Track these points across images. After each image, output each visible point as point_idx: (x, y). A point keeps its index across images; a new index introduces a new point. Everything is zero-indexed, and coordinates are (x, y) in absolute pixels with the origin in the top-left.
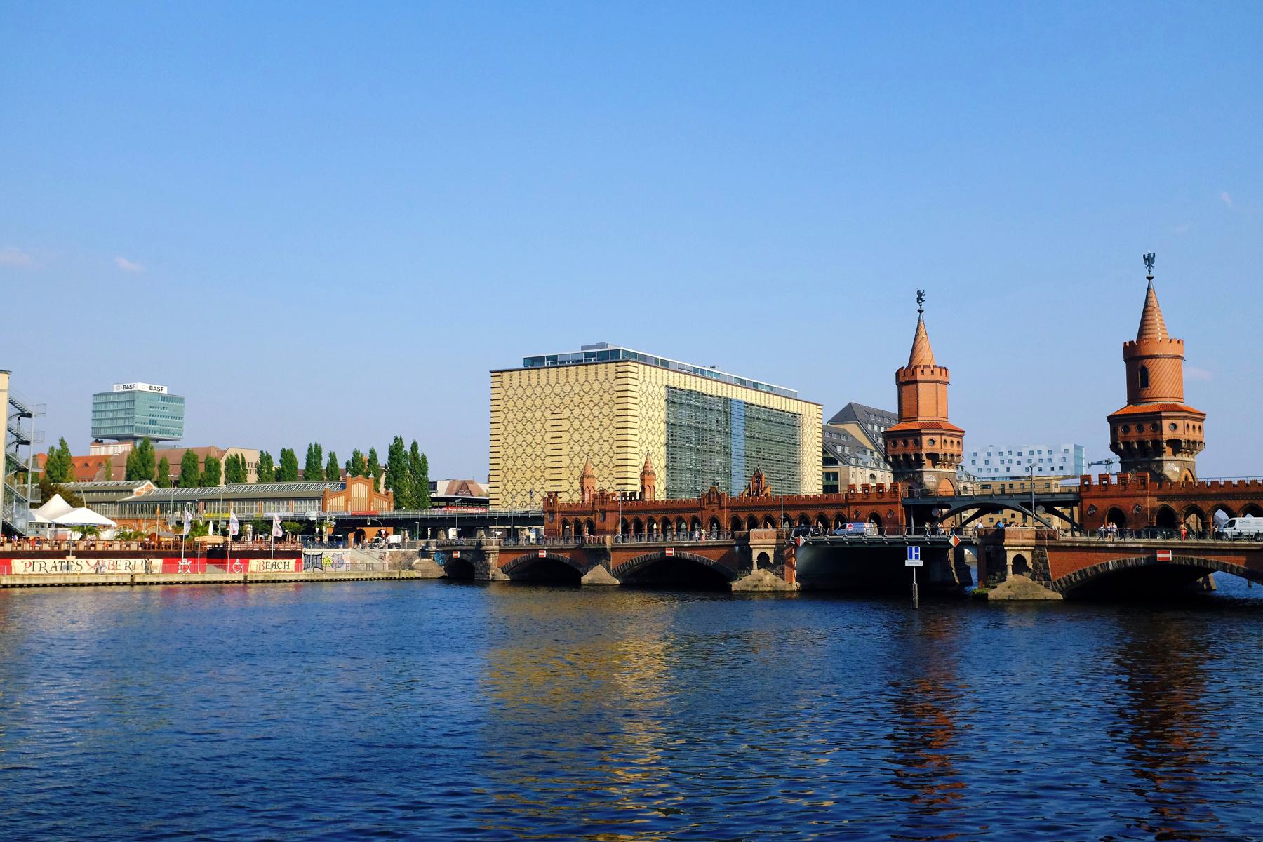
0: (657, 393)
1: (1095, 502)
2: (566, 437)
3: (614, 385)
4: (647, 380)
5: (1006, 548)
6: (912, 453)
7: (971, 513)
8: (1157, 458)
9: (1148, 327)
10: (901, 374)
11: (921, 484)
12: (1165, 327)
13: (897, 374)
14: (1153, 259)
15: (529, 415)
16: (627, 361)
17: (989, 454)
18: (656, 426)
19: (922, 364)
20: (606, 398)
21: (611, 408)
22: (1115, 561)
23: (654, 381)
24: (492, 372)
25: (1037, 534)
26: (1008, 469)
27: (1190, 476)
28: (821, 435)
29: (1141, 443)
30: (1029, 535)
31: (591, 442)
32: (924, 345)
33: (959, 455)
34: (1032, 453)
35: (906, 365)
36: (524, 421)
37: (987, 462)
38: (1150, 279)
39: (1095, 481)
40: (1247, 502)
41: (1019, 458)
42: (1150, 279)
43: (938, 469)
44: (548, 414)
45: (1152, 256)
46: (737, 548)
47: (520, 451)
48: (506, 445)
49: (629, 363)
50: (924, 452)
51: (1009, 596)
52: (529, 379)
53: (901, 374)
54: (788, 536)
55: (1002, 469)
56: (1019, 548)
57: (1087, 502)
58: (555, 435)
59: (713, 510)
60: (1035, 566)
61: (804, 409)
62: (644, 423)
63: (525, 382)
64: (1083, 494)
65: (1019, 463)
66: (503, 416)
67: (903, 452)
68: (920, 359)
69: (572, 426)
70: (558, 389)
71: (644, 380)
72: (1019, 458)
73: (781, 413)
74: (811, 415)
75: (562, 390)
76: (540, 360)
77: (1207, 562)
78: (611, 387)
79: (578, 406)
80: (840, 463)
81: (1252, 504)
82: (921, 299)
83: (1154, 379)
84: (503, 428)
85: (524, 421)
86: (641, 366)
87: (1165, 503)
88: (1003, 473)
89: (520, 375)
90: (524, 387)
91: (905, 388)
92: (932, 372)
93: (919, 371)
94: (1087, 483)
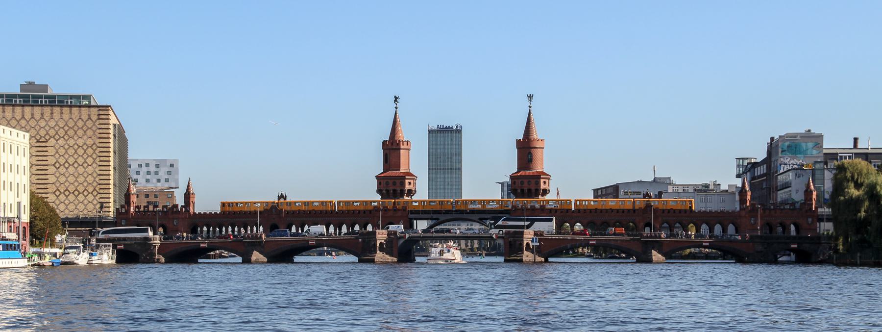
2: (51, 160)
3: (97, 123)
6: (399, 189)
12: (538, 133)
25: (535, 233)
34: (140, 166)
35: (387, 139)
38: (530, 107)
42: (530, 107)
46: (360, 240)
59: (274, 219)
69: (57, 152)
78: (94, 125)
79: (63, 137)
82: (397, 101)
90: (9, 119)
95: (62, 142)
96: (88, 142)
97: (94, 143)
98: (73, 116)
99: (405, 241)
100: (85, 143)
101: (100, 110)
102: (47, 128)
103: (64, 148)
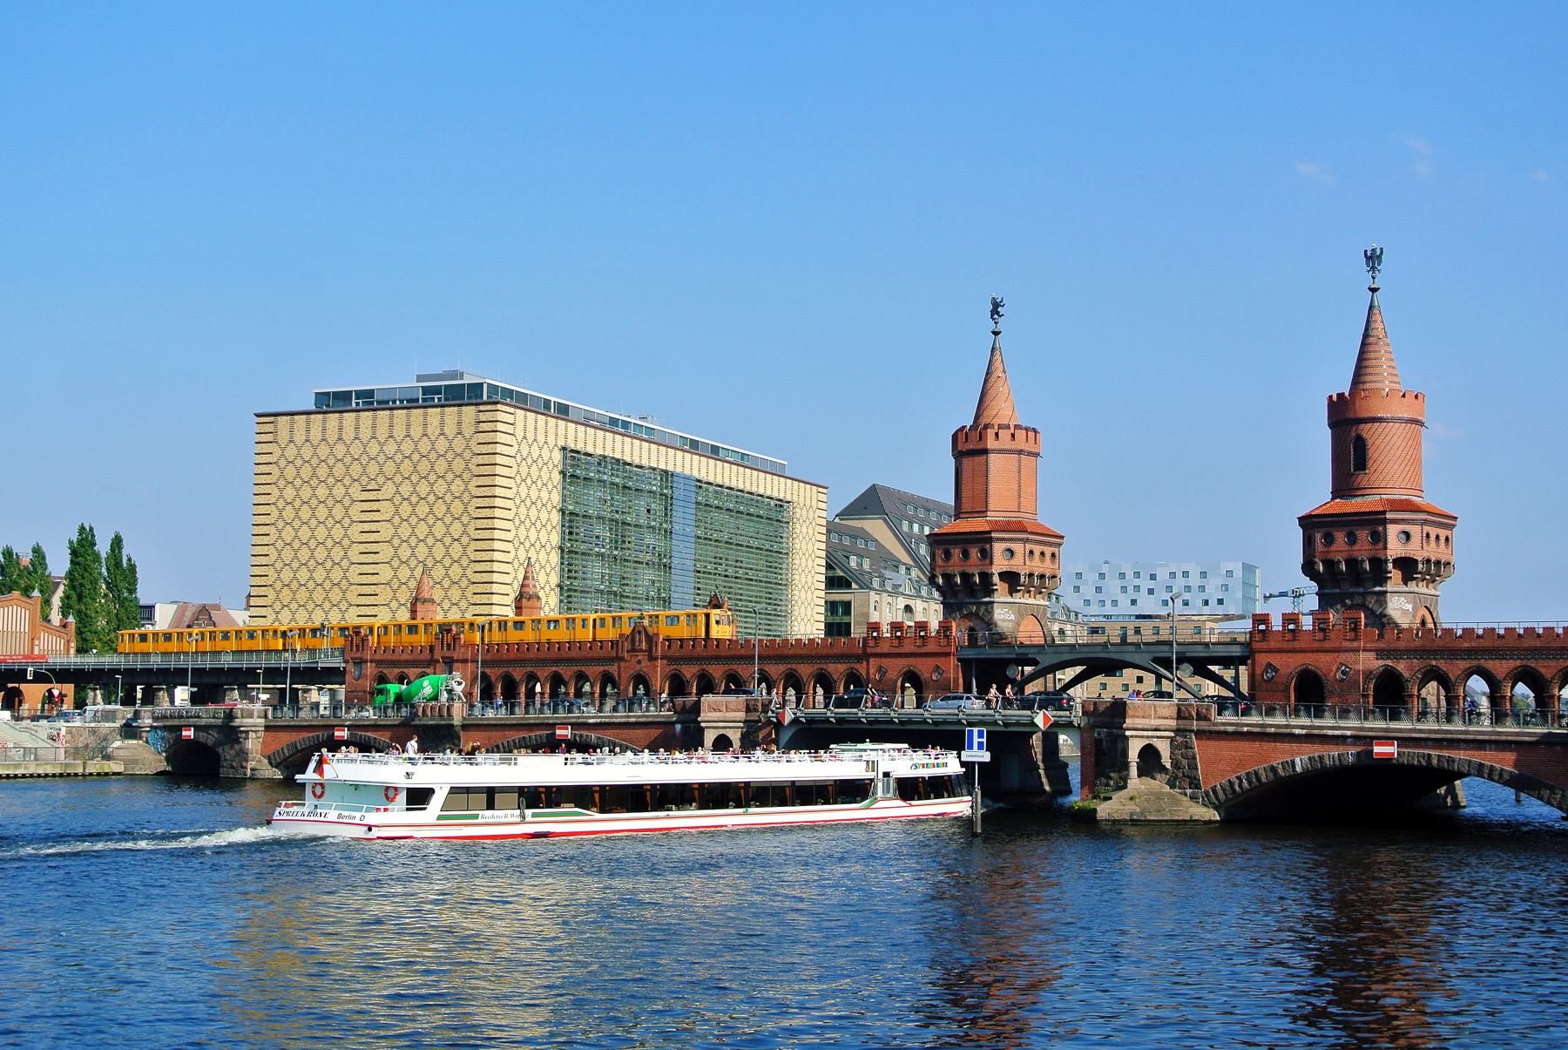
0: (546, 460)
1: (1276, 660)
2: (386, 531)
3: (473, 444)
4: (531, 437)
5: (1128, 733)
6: (976, 572)
7: (1069, 674)
8: (1378, 589)
9: (1368, 371)
10: (961, 438)
11: (990, 624)
13: (955, 437)
14: (1379, 257)
15: (322, 492)
16: (496, 403)
17: (1102, 576)
18: (544, 516)
19: (996, 422)
20: (459, 465)
21: (466, 484)
22: (1305, 758)
23: (541, 438)
24: (258, 415)
25: (1179, 711)
26: (1134, 602)
27: (1429, 619)
28: (824, 538)
29: (1352, 563)
30: (1166, 712)
31: (430, 541)
32: (1000, 389)
33: (1054, 577)
35: (969, 422)
36: (314, 502)
37: (1099, 590)
39: (1277, 624)
40: (1518, 663)
41: (1152, 584)
42: (1373, 290)
43: (1017, 598)
44: (355, 491)
45: (1378, 253)
46: (678, 727)
47: (304, 554)
48: (280, 544)
49: (499, 407)
50: (996, 570)
51: (1132, 814)
52: (324, 429)
53: (961, 438)
54: (766, 707)
55: (1124, 602)
56: (1150, 733)
57: (1262, 659)
58: (366, 527)
59: (639, 662)
60: (1176, 764)
61: (795, 493)
62: (523, 510)
63: (316, 434)
64: (1256, 646)
65: (1151, 592)
66: (276, 492)
67: (961, 569)
68: (994, 413)
70: (374, 449)
71: (525, 438)
72: (1152, 584)
73: (756, 498)
74: (808, 502)
75: (381, 451)
76: (344, 397)
77: (1453, 761)
78: (468, 447)
80: (854, 585)
81: (1527, 666)
82: (998, 313)
83: (1375, 456)
84: (275, 514)
85: (314, 502)
86: (520, 413)
87: (1389, 663)
88: (1125, 608)
89: (308, 422)
91: (967, 462)
92: (1013, 435)
93: (990, 433)
94: (1262, 627)
95: (406, 489)
96: (453, 488)
97: (466, 489)
98: (430, 431)
99: (1044, 733)
100: (449, 490)
101: (480, 411)
102: (381, 459)
103: (411, 504)
